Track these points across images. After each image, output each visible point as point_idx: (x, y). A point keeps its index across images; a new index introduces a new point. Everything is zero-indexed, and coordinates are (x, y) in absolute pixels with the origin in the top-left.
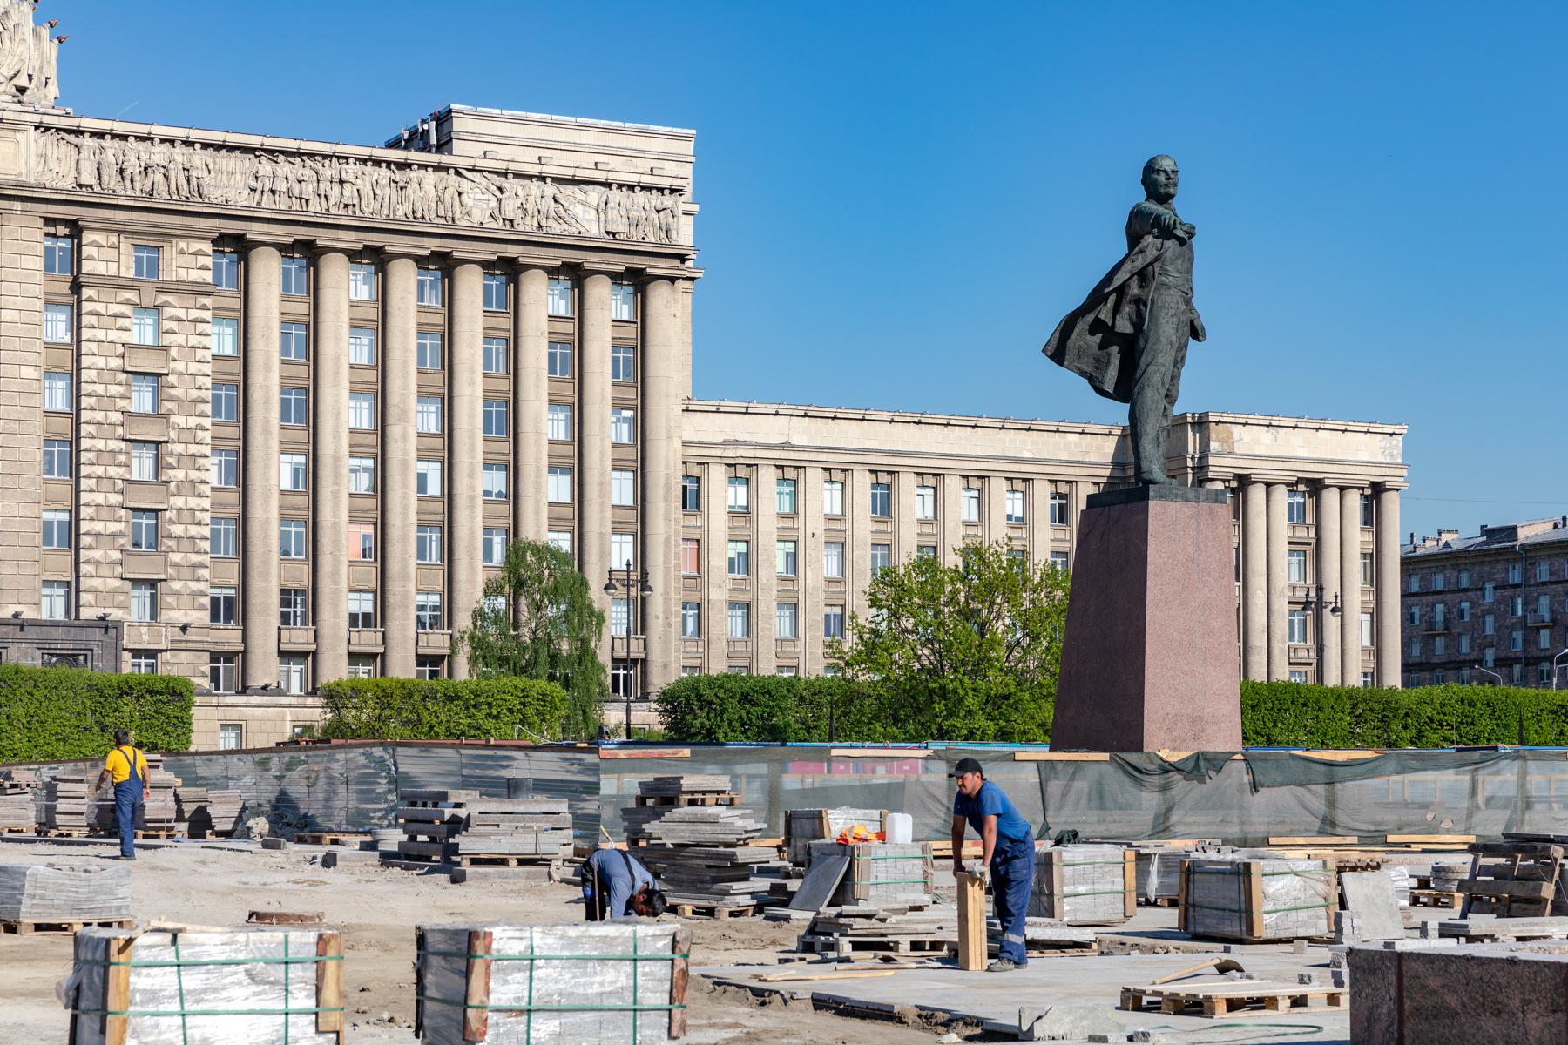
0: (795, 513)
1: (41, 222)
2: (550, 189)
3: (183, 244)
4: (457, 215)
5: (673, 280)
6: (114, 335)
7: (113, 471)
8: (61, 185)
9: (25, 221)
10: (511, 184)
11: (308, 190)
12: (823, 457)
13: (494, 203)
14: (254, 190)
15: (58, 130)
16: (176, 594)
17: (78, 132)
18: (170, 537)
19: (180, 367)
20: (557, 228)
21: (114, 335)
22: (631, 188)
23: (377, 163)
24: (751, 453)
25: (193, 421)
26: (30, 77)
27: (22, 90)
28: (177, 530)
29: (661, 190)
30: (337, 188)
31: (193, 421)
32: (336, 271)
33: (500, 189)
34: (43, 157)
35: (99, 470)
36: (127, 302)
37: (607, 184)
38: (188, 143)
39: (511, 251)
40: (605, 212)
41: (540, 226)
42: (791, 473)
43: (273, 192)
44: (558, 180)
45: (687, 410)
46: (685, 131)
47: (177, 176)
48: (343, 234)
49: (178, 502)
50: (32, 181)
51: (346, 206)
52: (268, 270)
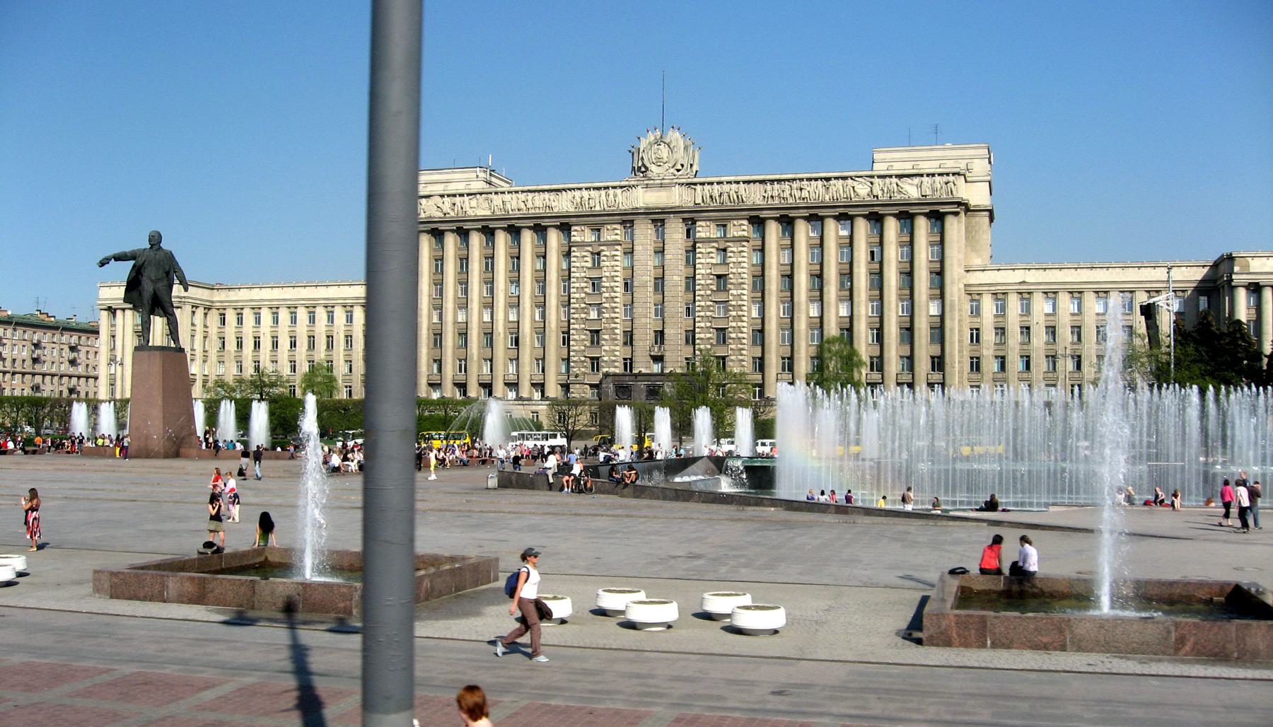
0: (1054, 314)
1: (681, 220)
2: (894, 180)
3: (735, 222)
4: (853, 196)
5: (956, 214)
6: (708, 260)
7: (709, 314)
8: (689, 205)
9: (675, 220)
10: (876, 180)
11: (787, 194)
12: (1042, 287)
13: (869, 189)
14: (764, 197)
15: (687, 184)
16: (732, 361)
17: (695, 184)
18: (730, 338)
19: (734, 270)
20: (897, 197)
21: (708, 260)
22: (933, 175)
23: (816, 179)
24: (1004, 288)
25: (739, 292)
26: (682, 166)
27: (678, 170)
28: (733, 335)
29: (948, 174)
30: (799, 191)
31: (739, 292)
32: (831, 225)
33: (872, 183)
34: (681, 196)
35: (702, 314)
36: (713, 247)
37: (922, 175)
38: (738, 182)
39: (876, 209)
40: (921, 186)
41: (891, 197)
42: (1026, 296)
43: (772, 197)
44: (900, 177)
45: (968, 271)
46: (983, 145)
47: (732, 193)
48: (801, 211)
49: (734, 324)
50: (677, 205)
51: (804, 199)
52: (773, 229)
